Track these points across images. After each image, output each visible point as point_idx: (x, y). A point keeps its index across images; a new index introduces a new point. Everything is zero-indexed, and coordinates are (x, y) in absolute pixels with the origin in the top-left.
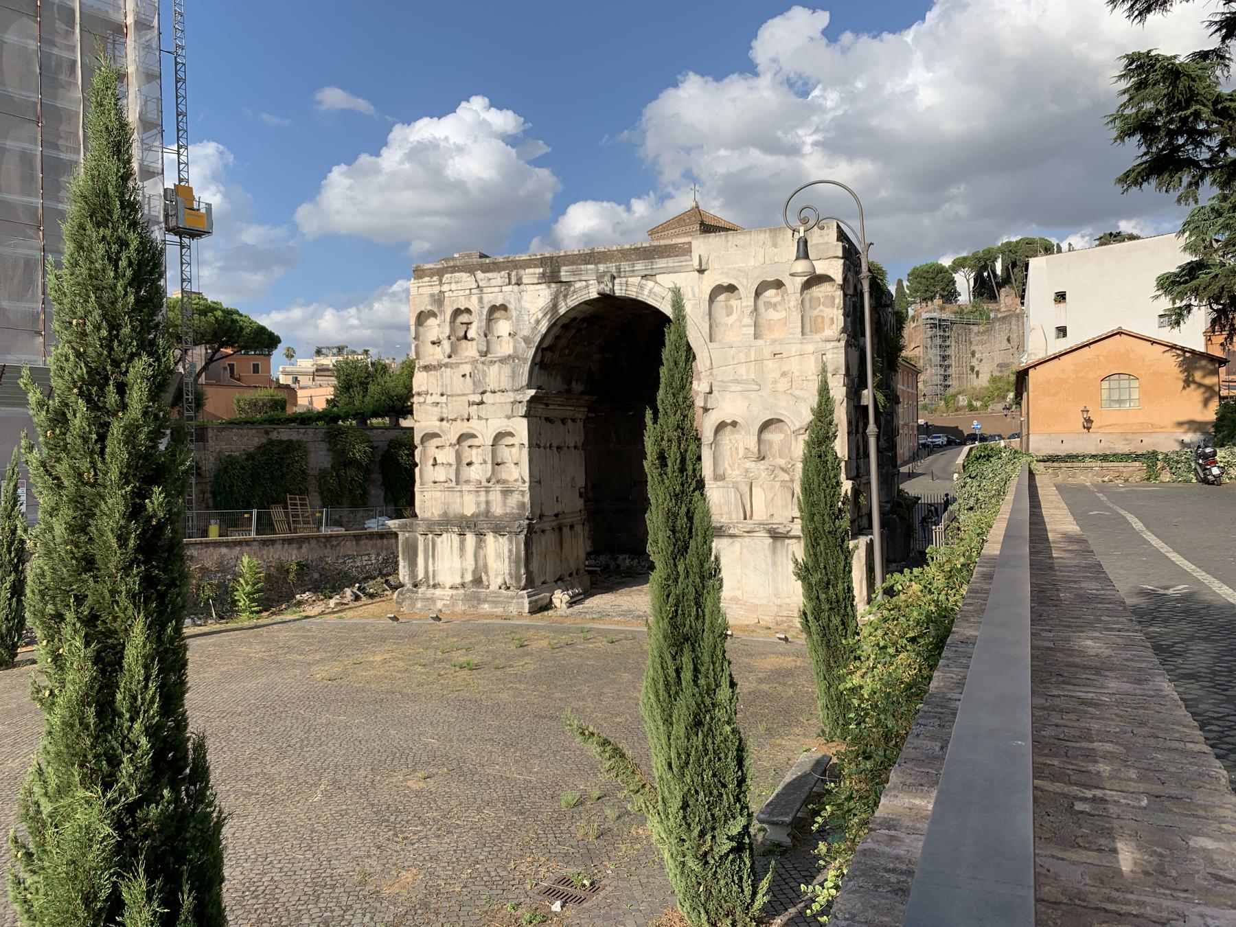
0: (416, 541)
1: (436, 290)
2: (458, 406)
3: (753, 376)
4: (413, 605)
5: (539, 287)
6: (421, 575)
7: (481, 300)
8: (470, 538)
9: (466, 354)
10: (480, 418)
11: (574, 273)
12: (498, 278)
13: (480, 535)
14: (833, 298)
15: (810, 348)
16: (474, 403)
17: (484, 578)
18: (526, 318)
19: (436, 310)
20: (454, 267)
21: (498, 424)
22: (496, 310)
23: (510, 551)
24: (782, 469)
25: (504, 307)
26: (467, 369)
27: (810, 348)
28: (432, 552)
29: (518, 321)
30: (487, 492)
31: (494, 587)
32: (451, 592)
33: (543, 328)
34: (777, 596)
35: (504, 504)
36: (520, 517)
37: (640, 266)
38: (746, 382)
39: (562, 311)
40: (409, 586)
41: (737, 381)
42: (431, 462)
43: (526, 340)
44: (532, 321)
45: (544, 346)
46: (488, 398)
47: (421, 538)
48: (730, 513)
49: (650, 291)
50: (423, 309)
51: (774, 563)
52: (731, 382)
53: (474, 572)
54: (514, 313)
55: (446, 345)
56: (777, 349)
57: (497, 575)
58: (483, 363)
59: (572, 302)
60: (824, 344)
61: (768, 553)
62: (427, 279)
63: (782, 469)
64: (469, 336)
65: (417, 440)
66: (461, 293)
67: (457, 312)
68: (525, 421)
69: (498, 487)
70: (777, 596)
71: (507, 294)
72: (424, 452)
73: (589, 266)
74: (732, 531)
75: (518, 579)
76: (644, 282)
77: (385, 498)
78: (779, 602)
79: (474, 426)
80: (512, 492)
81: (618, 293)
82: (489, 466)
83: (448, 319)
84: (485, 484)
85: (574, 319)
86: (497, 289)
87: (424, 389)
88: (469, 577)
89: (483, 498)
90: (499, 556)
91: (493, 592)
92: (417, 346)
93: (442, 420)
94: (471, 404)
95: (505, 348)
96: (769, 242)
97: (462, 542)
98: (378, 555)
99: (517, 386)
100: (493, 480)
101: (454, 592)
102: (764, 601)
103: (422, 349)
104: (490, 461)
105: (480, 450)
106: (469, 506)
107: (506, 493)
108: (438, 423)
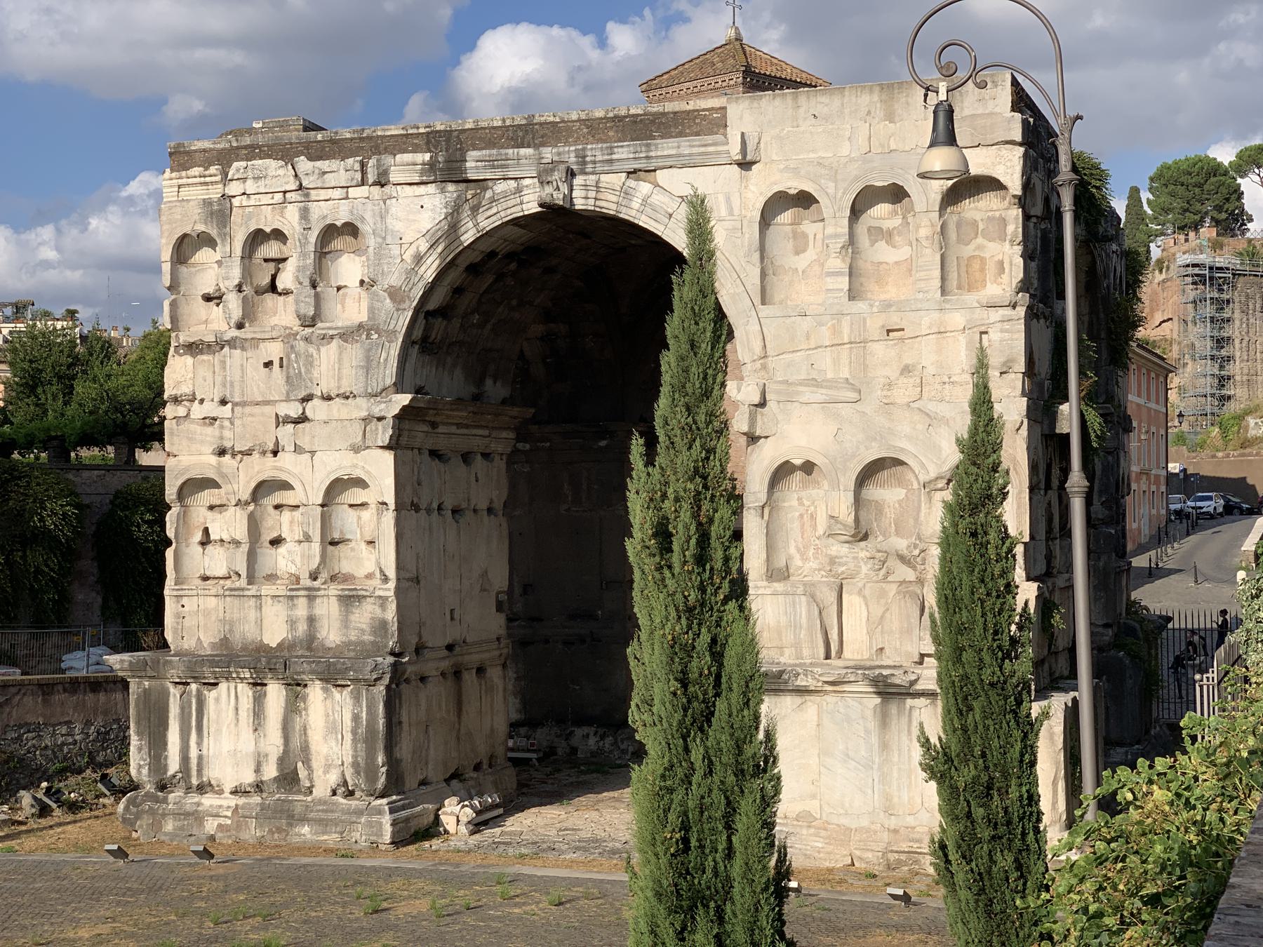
0: (165, 695)
1: (215, 193)
2: (255, 426)
3: (845, 373)
4: (156, 826)
5: (422, 190)
6: (173, 765)
7: (305, 214)
8: (275, 693)
9: (275, 321)
10: (298, 449)
11: (492, 164)
12: (340, 171)
13: (295, 686)
14: (1003, 222)
15: (957, 319)
16: (288, 420)
17: (302, 773)
18: (396, 251)
19: (214, 232)
20: (252, 147)
21: (334, 462)
22: (335, 235)
23: (356, 718)
24: (902, 558)
25: (351, 229)
26: (274, 350)
27: (957, 319)
28: (195, 721)
29: (379, 255)
30: (311, 599)
31: (321, 791)
32: (233, 801)
33: (429, 270)
34: (889, 811)
35: (346, 623)
36: (376, 649)
37: (623, 152)
38: (832, 384)
39: (468, 237)
40: (149, 787)
41: (814, 383)
42: (198, 536)
43: (394, 294)
44: (408, 257)
45: (431, 306)
46: (316, 409)
47: (174, 692)
48: (797, 646)
49: (645, 202)
50: (187, 229)
51: (885, 746)
52: (802, 383)
53: (281, 761)
54: (372, 242)
56: (894, 320)
57: (328, 768)
58: (307, 339)
59: (489, 220)
60: (984, 313)
61: (872, 724)
62: (196, 171)
63: (902, 558)
64: (280, 285)
65: (170, 493)
66: (266, 199)
67: (257, 238)
68: (389, 457)
69: (334, 590)
70: (889, 811)
71: (357, 204)
72: (184, 517)
73: (523, 151)
74: (801, 682)
75: (371, 775)
76: (631, 183)
77: (104, 607)
78: (893, 823)
79: (287, 465)
80: (360, 598)
81: (579, 204)
82: (316, 547)
83: (238, 251)
84: (309, 583)
85: (492, 254)
86: (338, 193)
87: (185, 389)
88: (270, 772)
89: (301, 610)
90: (332, 728)
91: (321, 802)
92: (174, 305)
93: (222, 452)
94: (280, 421)
95: (351, 309)
96: (879, 112)
97: (259, 701)
98: (88, 723)
99: (375, 386)
100: (324, 576)
101: (241, 801)
102: (865, 822)
103: (184, 310)
104: (316, 536)
105: (297, 514)
106: (274, 627)
107: (349, 600)
108: (214, 460)
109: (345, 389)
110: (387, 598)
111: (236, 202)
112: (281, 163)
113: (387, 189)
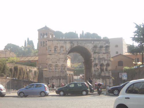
8: (58, 80)
10: (59, 62)
13: (60, 79)
22: (62, 47)
26: (57, 55)
33: (70, 49)
37: (84, 42)
43: (67, 51)
44: (68, 49)
46: (60, 59)
55: (53, 51)
59: (74, 46)
67: (55, 46)
79: (58, 63)
88: (58, 85)
93: (52, 62)
109: (63, 58)
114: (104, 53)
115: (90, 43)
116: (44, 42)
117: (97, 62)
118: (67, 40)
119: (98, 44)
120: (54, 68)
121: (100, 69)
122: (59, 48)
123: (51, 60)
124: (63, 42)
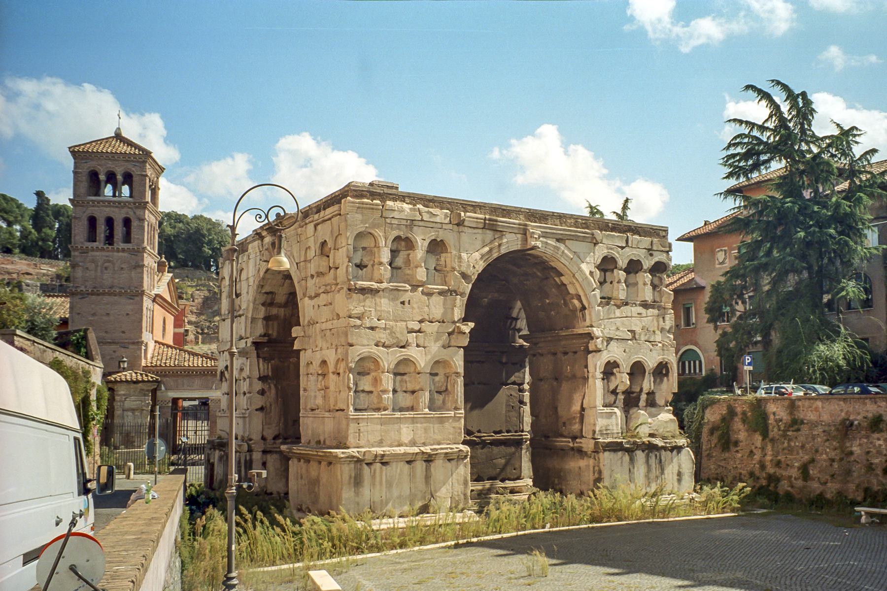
8: (420, 466)
10: (418, 346)
26: (406, 297)
39: (495, 255)
43: (464, 276)
62: (366, 200)
79: (413, 352)
86: (440, 226)
93: (377, 345)
94: (411, 331)
105: (405, 377)
110: (460, 417)
111: (388, 221)
112: (411, 206)
113: (461, 228)
114: (645, 305)
115: (583, 239)
116: (110, 222)
117: (615, 352)
118: (467, 206)
119: (622, 248)
120: (388, 382)
121: (621, 397)
122: (420, 253)
123: (372, 328)
124: (441, 215)
